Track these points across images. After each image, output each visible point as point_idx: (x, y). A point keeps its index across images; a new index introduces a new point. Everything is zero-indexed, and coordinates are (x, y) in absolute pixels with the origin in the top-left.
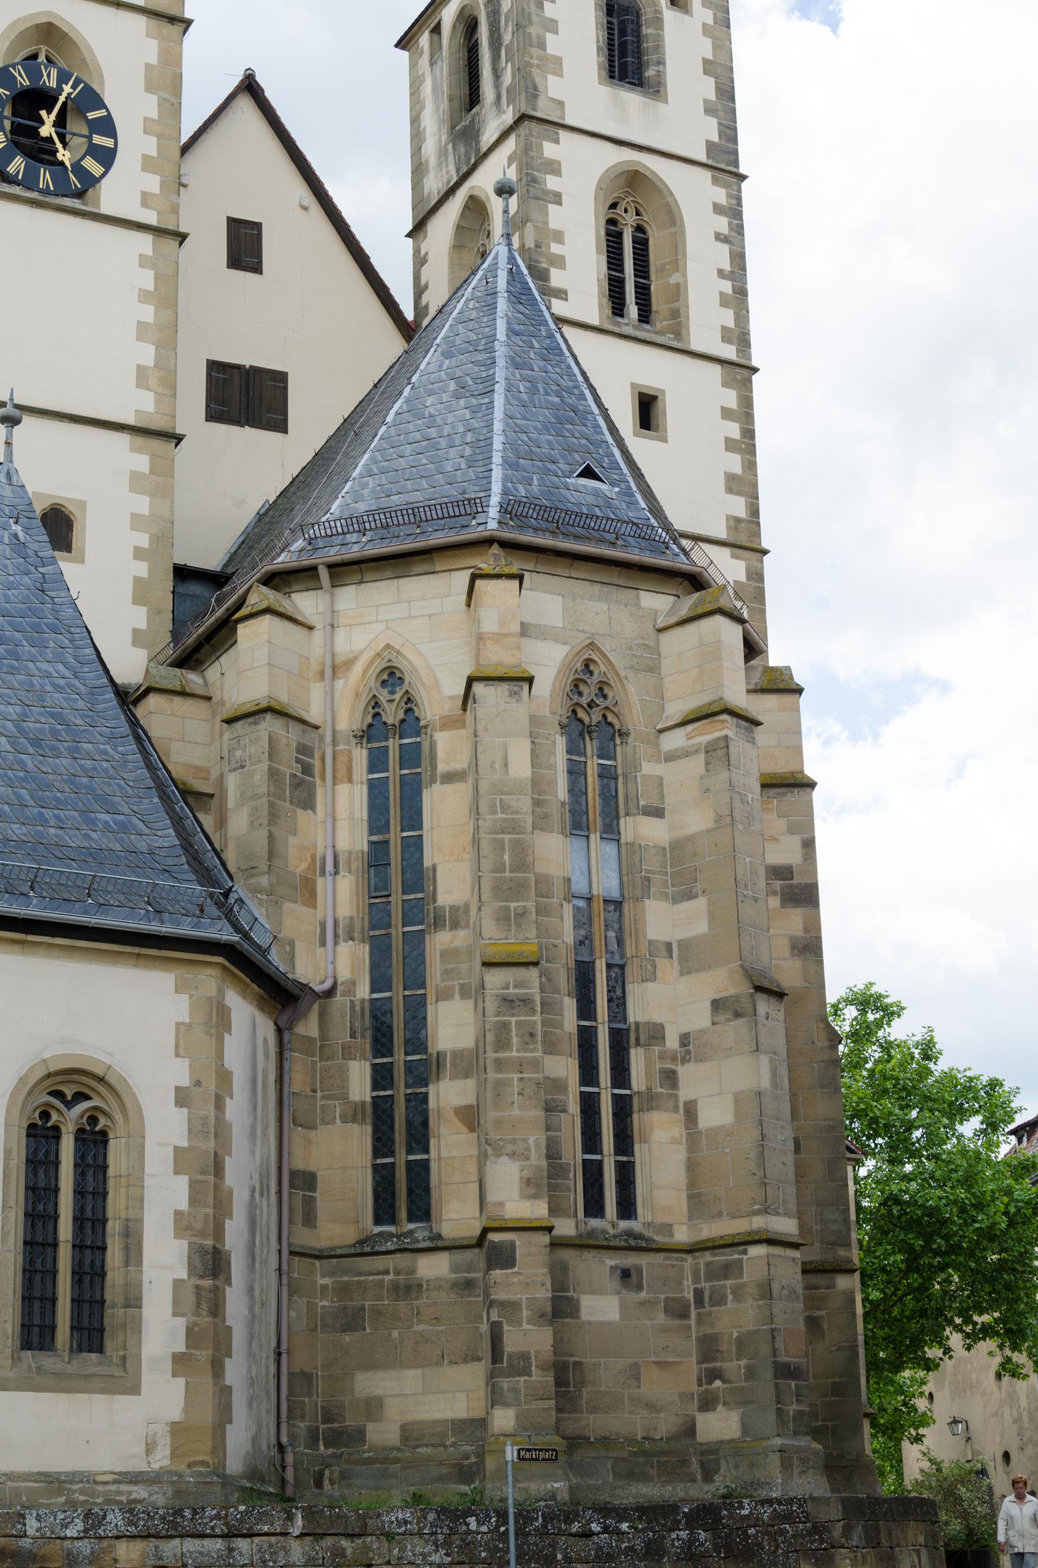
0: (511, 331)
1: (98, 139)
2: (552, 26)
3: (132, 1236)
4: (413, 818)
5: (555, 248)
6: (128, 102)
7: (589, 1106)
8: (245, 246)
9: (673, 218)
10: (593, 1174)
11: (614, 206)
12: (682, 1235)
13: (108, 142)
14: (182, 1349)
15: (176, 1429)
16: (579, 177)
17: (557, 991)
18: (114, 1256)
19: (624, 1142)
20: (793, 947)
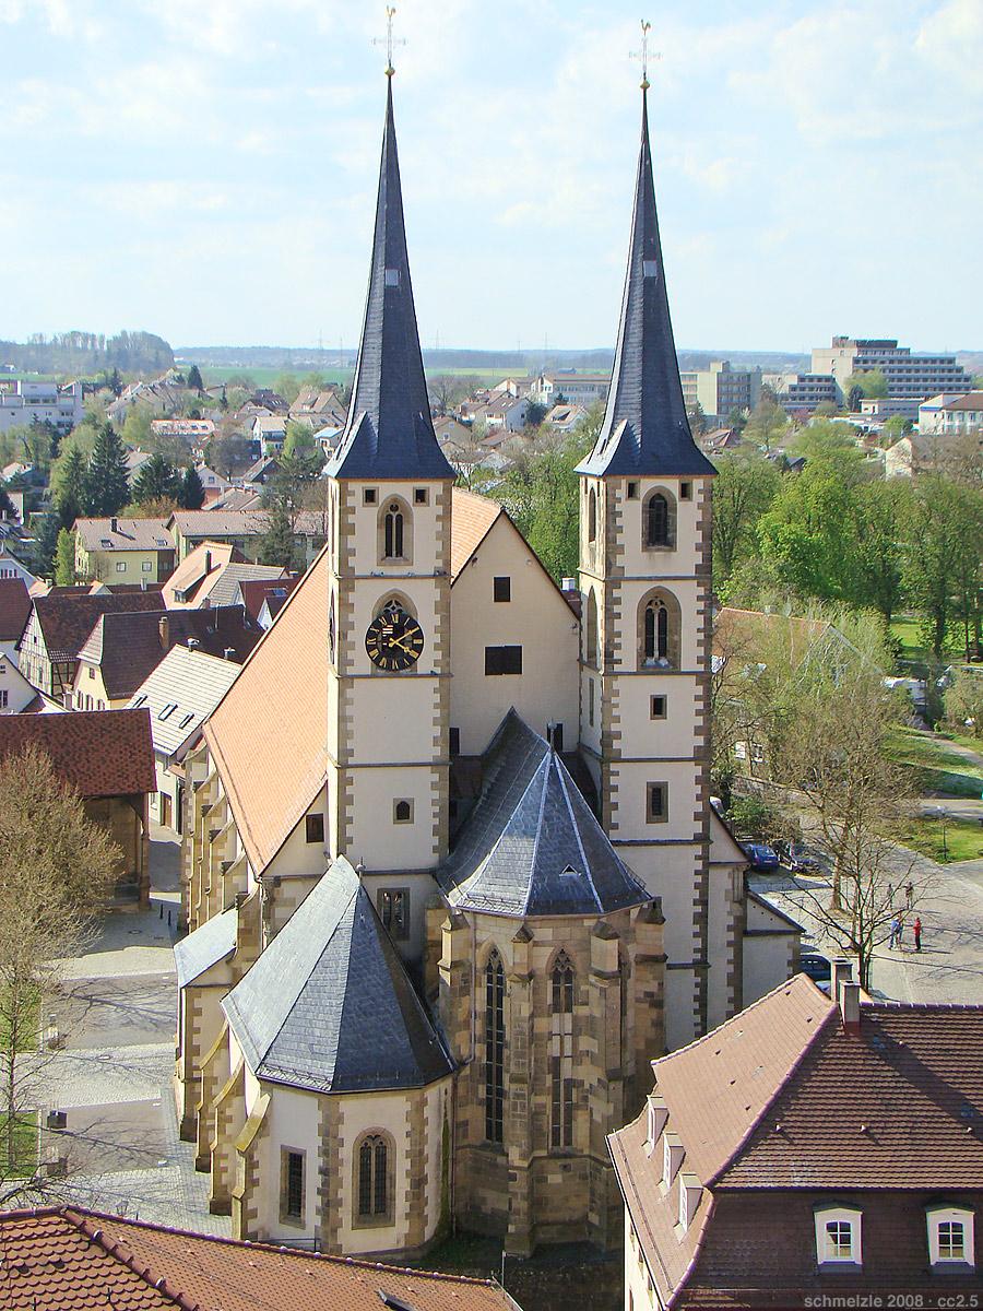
0: (547, 801)
1: (415, 642)
2: (620, 529)
3: (393, 1179)
4: (500, 1004)
5: (617, 640)
6: (428, 620)
7: (556, 1110)
8: (502, 590)
9: (677, 609)
10: (556, 1132)
11: (650, 603)
12: (586, 1152)
13: (420, 642)
14: (408, 1211)
15: (406, 1235)
16: (632, 597)
17: (544, 1073)
18: (388, 1185)
19: (569, 1119)
20: (653, 1023)
